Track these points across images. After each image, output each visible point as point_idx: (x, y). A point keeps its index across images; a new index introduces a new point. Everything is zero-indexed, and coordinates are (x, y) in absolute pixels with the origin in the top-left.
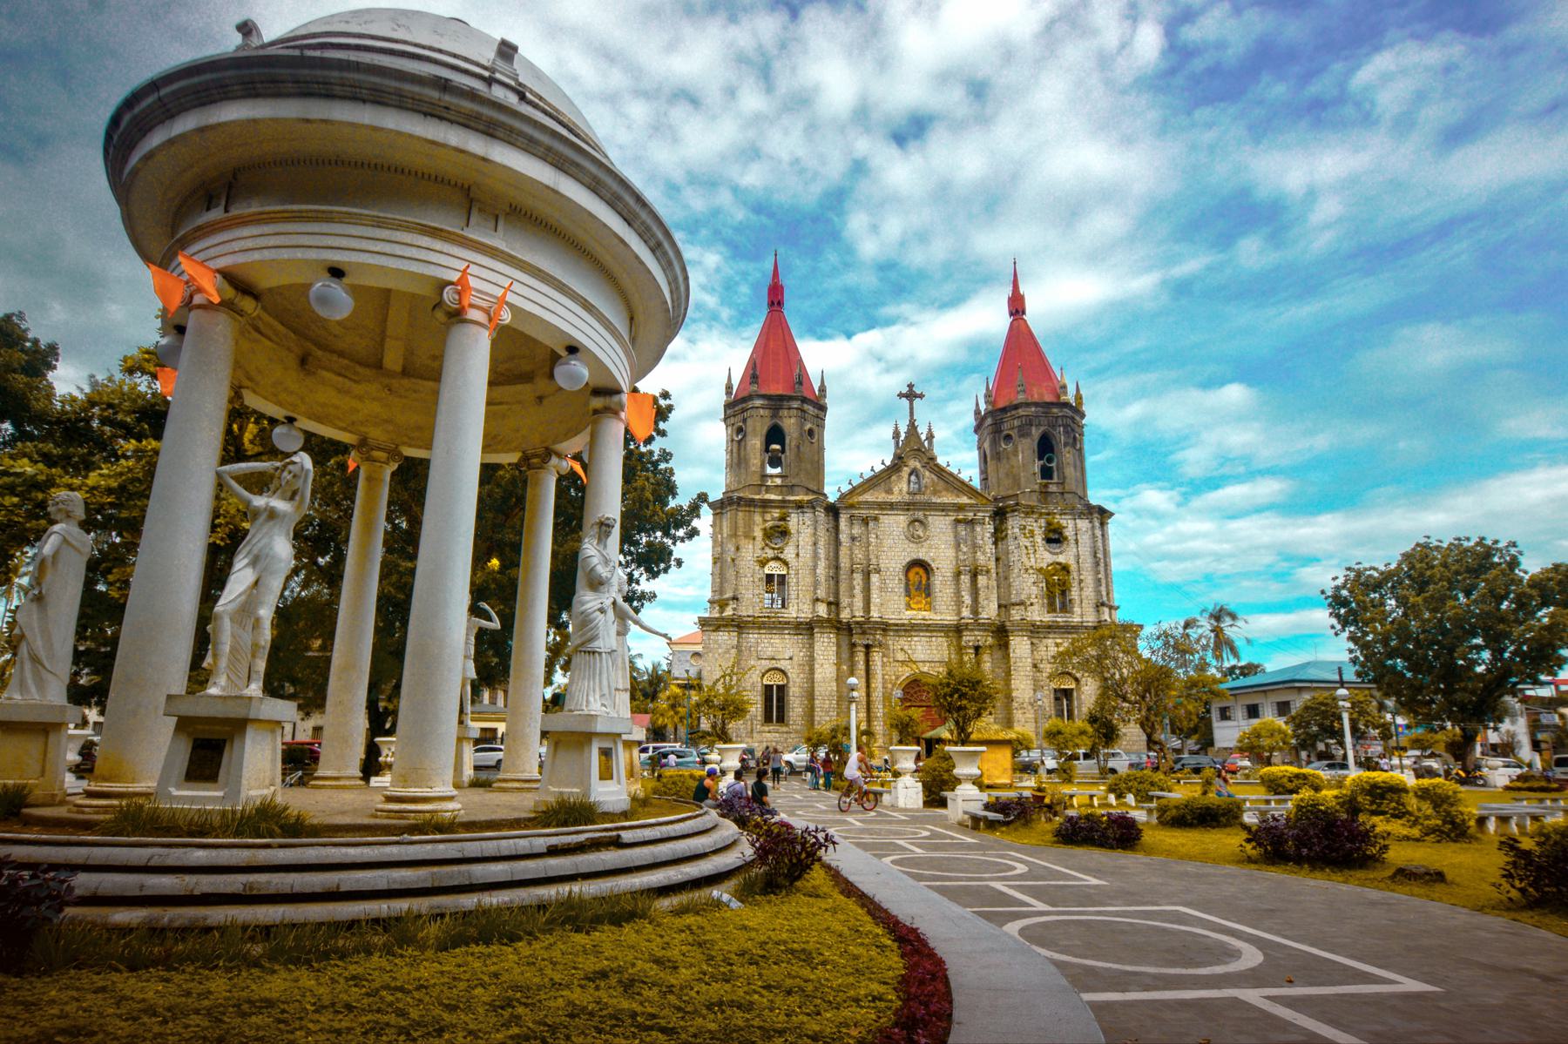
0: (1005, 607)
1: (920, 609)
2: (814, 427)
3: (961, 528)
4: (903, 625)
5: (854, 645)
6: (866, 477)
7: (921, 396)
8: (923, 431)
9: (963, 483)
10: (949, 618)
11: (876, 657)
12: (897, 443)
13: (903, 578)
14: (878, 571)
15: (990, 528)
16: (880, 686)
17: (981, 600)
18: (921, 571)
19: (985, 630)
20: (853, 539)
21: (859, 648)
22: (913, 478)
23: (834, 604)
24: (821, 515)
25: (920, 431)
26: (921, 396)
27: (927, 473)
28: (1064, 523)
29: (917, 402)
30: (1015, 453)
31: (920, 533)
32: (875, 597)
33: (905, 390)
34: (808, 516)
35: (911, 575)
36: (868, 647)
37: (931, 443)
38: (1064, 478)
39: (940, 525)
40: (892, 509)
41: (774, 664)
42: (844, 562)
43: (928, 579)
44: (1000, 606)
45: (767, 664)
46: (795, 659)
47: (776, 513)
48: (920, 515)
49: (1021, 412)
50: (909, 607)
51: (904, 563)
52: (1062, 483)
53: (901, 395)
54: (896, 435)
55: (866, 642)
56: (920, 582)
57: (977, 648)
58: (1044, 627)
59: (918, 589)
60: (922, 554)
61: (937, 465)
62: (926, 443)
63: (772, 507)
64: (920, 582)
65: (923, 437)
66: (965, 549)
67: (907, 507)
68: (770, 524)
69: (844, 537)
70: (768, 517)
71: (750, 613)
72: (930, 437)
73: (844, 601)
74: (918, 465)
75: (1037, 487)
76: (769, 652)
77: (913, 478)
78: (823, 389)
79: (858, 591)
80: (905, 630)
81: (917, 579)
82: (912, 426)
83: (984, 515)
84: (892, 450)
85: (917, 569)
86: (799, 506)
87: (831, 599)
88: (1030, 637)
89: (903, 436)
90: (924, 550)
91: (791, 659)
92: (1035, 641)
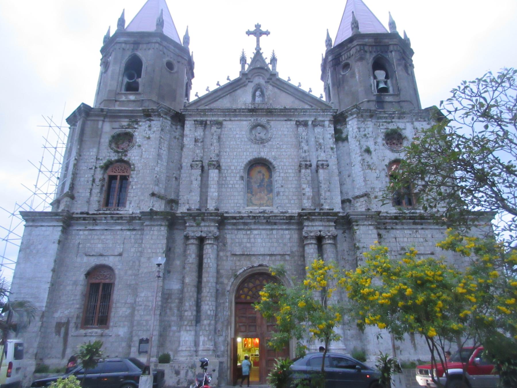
0: (349, 201)
1: (261, 205)
2: (175, 63)
3: (301, 129)
4: (242, 218)
5: (187, 238)
6: (212, 89)
7: (267, 33)
8: (267, 56)
9: (303, 93)
10: (294, 211)
11: (209, 251)
12: (243, 67)
13: (245, 176)
14: (218, 167)
15: (331, 130)
16: (213, 280)
17: (323, 192)
18: (264, 170)
19: (329, 221)
20: (196, 141)
21: (192, 241)
22: (258, 93)
23: (173, 202)
24: (168, 123)
25: (264, 56)
26: (267, 33)
27: (270, 87)
28: (401, 125)
29: (263, 38)
30: (353, 75)
31: (262, 135)
32: (213, 192)
33: (253, 29)
34: (156, 124)
36: (201, 240)
37: (274, 66)
38: (399, 90)
40: (236, 116)
42: (186, 162)
43: (271, 176)
44: (343, 202)
45: (94, 261)
46: (125, 255)
47: (125, 122)
48: (263, 120)
49: (355, 43)
50: (249, 202)
51: (246, 161)
52: (398, 95)
53: (249, 33)
54: (243, 60)
55: (199, 234)
56: (262, 180)
57: (320, 239)
58: (391, 218)
59: (260, 185)
60: (264, 153)
61: (279, 80)
62: (270, 66)
63: (120, 117)
64: (262, 180)
65: (268, 61)
66: (306, 148)
67: (253, 111)
68: (118, 131)
69: (186, 141)
70: (116, 125)
71: (85, 210)
72: (274, 60)
73: (184, 197)
74: (262, 81)
75: (374, 98)
76: (99, 247)
77: (258, 93)
78: (187, 38)
79: (196, 184)
80: (245, 224)
81: (259, 177)
82: (258, 54)
83: (327, 119)
84: (239, 68)
85: (259, 168)
86: (148, 115)
87: (173, 197)
88: (378, 228)
89: (249, 61)
90: (266, 150)
91: (120, 255)
92: (382, 232)
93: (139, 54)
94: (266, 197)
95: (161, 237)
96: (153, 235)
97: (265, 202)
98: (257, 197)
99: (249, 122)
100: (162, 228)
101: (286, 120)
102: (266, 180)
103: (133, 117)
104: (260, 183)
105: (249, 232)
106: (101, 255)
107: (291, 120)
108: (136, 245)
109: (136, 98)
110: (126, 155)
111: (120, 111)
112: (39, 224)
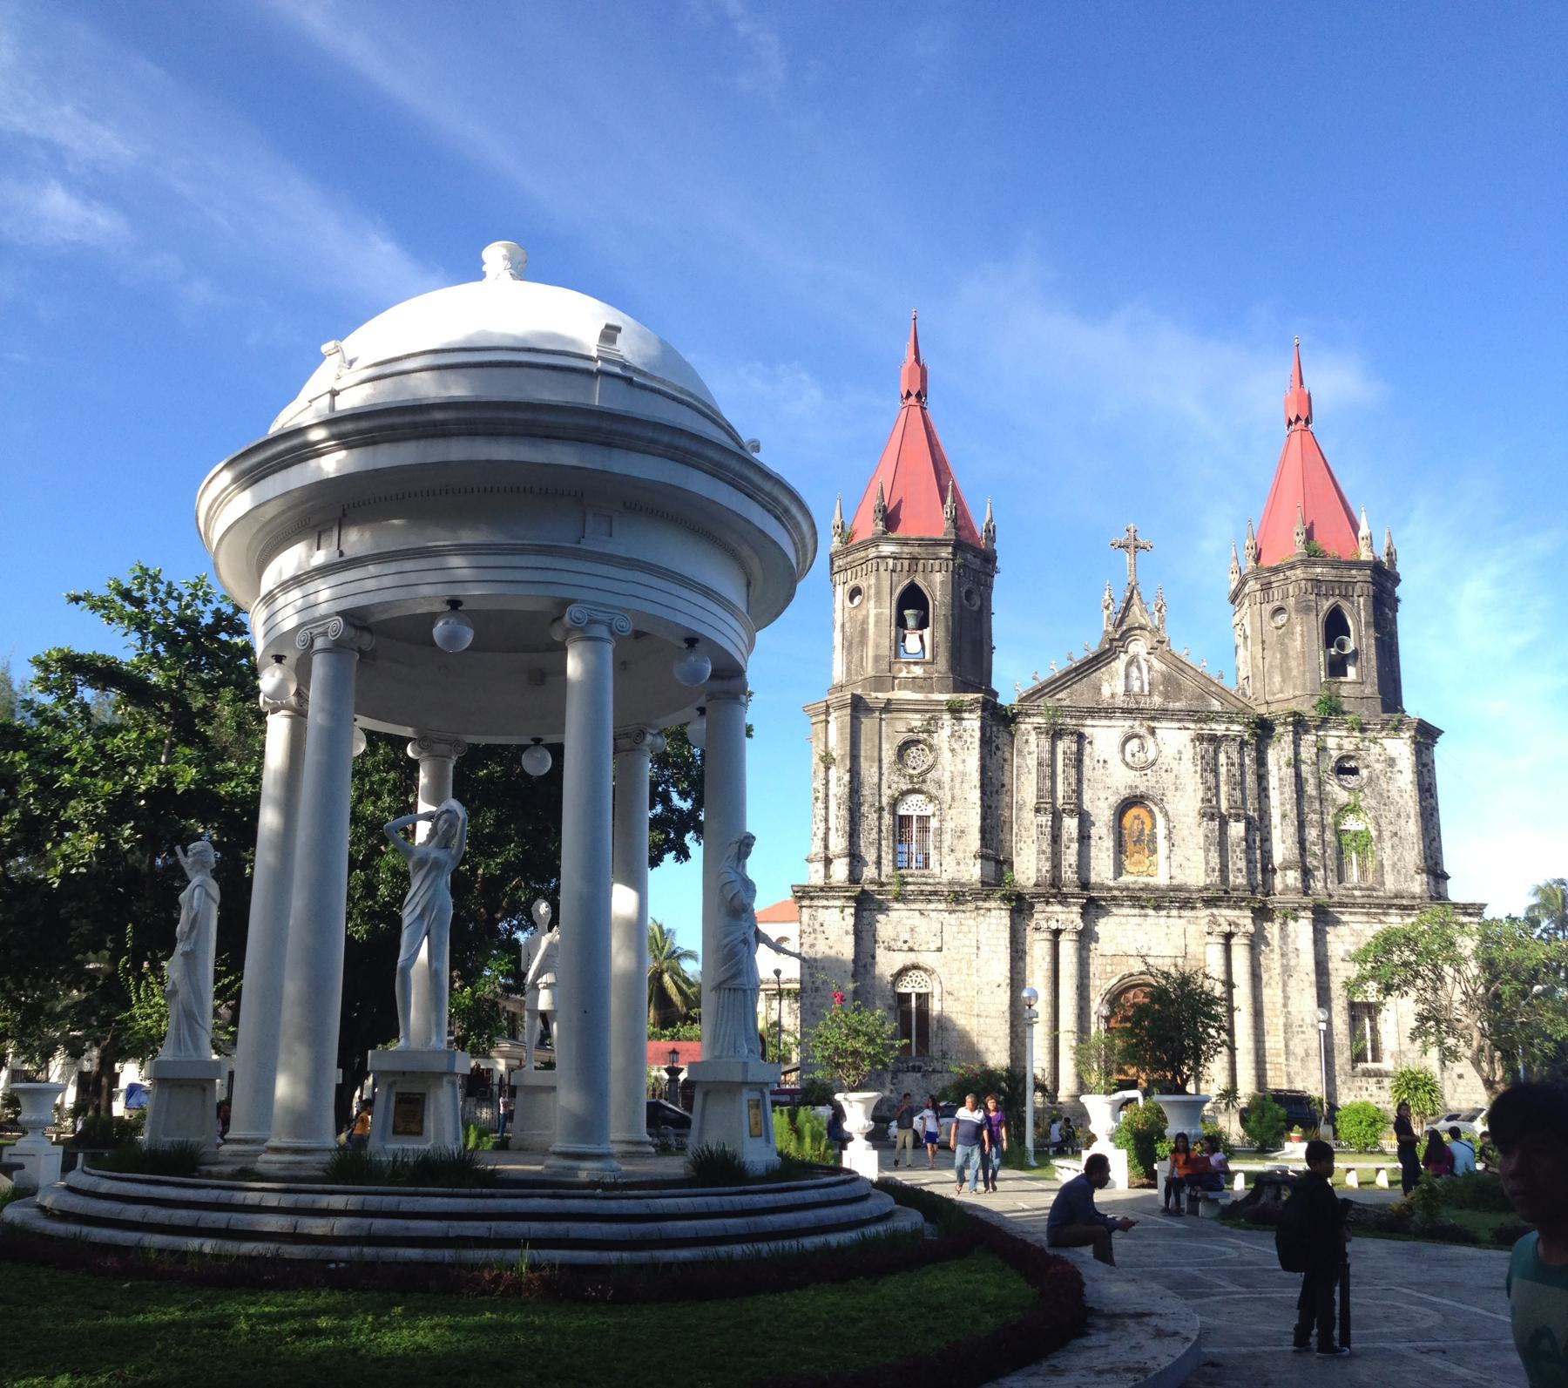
35: (1128, 819)
39: (1175, 741)
41: (910, 959)
59: (1138, 841)
81: (1136, 826)
85: (1134, 812)
93: (920, 581)
94: (1147, 862)
95: (1002, 928)
96: (989, 924)
97: (1145, 869)
98: (1133, 859)
99: (1122, 729)
100: (1003, 913)
101: (1180, 729)
102: (1147, 832)
103: (927, 711)
104: (1138, 836)
105: (1124, 920)
106: (911, 950)
107: (1189, 729)
108: (961, 936)
109: (925, 671)
110: (924, 781)
111: (908, 702)
112: (820, 905)
